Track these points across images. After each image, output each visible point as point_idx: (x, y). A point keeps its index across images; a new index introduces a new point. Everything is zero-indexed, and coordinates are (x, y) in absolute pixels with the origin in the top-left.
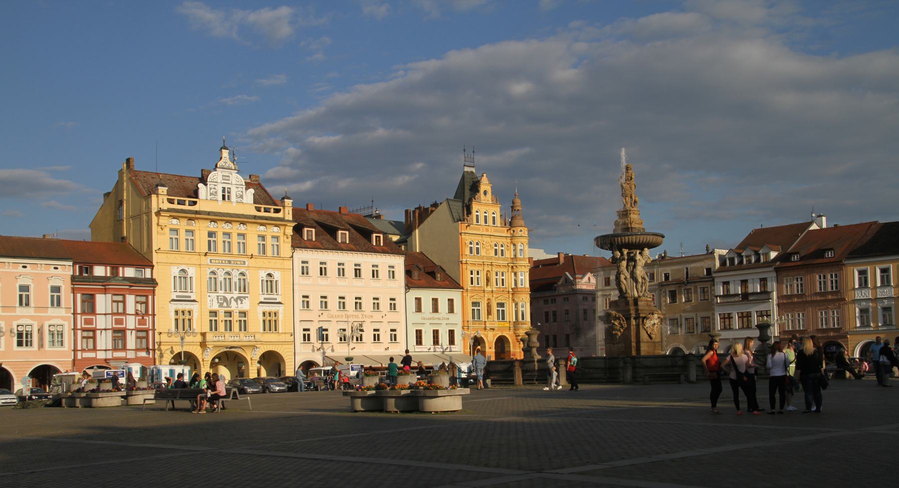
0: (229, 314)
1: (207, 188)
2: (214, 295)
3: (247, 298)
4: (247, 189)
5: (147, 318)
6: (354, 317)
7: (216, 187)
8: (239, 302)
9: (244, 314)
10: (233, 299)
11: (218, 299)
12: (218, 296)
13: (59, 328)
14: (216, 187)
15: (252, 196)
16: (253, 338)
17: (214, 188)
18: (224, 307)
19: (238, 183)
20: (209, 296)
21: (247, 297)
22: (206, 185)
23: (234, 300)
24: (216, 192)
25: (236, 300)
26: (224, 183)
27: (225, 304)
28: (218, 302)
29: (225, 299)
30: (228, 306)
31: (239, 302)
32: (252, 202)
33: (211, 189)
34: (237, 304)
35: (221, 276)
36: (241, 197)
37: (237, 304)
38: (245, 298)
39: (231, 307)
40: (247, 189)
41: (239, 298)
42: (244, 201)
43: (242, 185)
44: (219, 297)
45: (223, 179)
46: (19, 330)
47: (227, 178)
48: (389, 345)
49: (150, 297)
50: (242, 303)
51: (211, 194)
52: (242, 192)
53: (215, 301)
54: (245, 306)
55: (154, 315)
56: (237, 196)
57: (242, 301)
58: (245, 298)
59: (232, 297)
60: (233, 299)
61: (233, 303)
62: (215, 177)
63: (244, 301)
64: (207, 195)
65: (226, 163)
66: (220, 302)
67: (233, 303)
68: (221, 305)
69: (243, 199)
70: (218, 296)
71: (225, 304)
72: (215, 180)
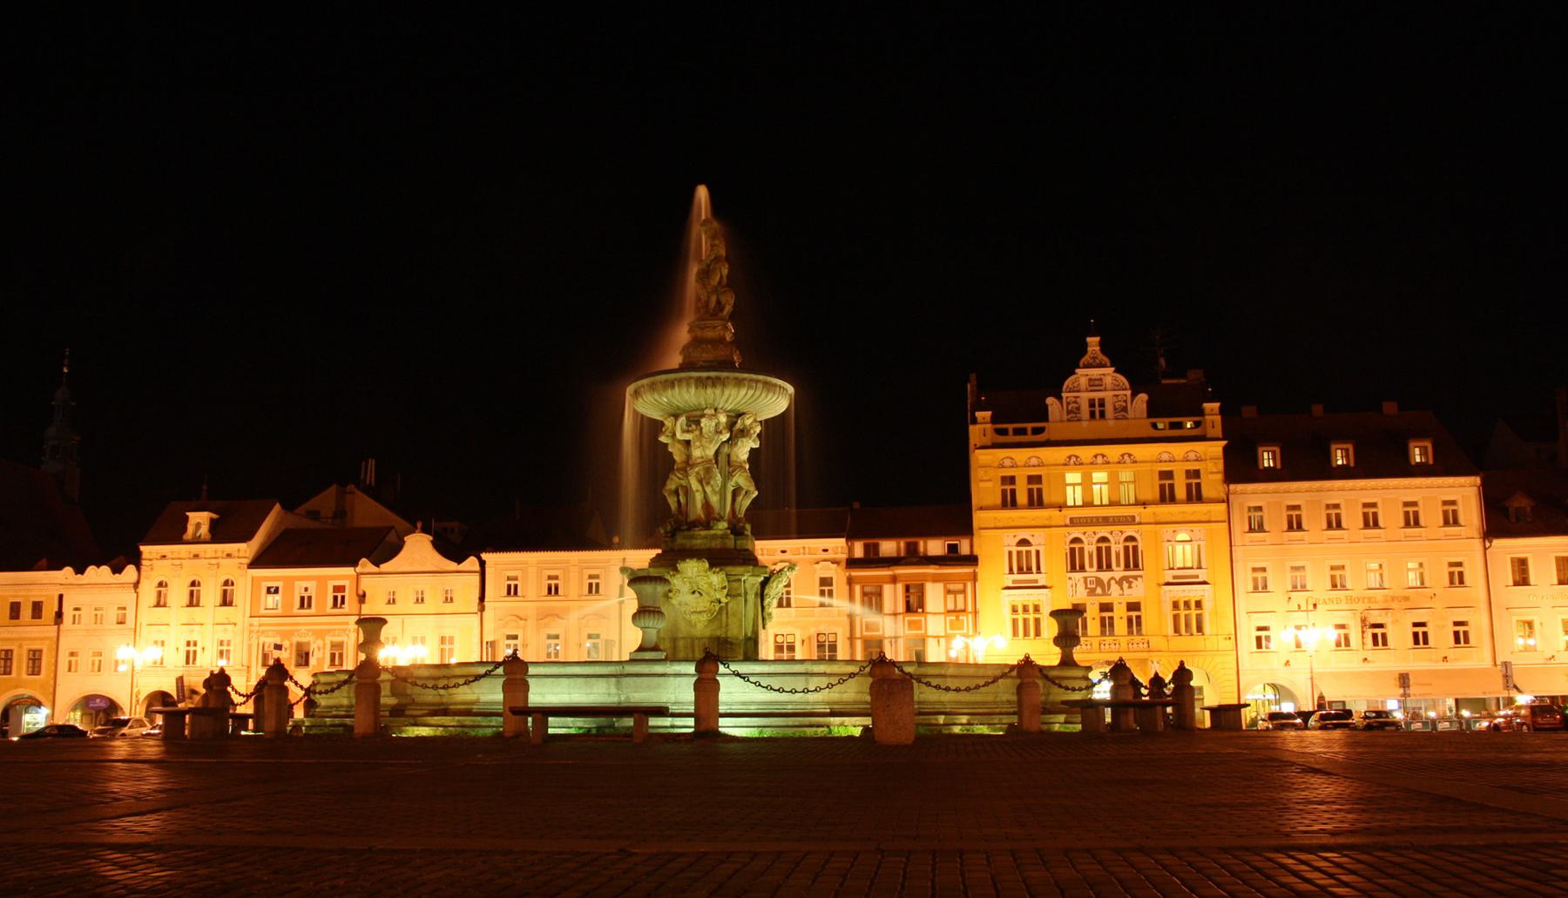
0: (1106, 607)
1: (1062, 403)
2: (1078, 576)
3: (1139, 579)
4: (1134, 395)
5: (965, 618)
6: (1366, 601)
7: (1078, 400)
8: (1125, 585)
9: (1133, 606)
10: (1113, 582)
11: (1085, 582)
12: (1085, 578)
13: (790, 639)
14: (1078, 400)
15: (1145, 405)
16: (1146, 645)
17: (1075, 402)
18: (1098, 595)
19: (1117, 388)
20: (1070, 578)
21: (1141, 576)
22: (1060, 398)
23: (1116, 582)
24: (1078, 409)
25: (1120, 583)
26: (1092, 391)
27: (1099, 591)
28: (1086, 588)
29: (1099, 582)
30: (1104, 593)
31: (1125, 585)
32: (1145, 415)
33: (1068, 404)
34: (1122, 589)
35: (1090, 547)
36: (1125, 409)
37: (1122, 589)
38: (1136, 578)
39: (1110, 595)
40: (1134, 395)
41: (1124, 578)
42: (1131, 414)
43: (1126, 389)
44: (1089, 579)
45: (1090, 386)
46: (820, 640)
47: (1097, 383)
48: (1451, 654)
49: (969, 585)
50: (1130, 587)
51: (1069, 412)
52: (1125, 401)
53: (1081, 588)
54: (1136, 593)
55: (975, 612)
56: (1115, 409)
57: (1130, 583)
58: (1136, 578)
59: (1113, 578)
60: (1113, 582)
61: (1114, 587)
62: (1076, 385)
63: (1135, 583)
64: (1061, 415)
65: (1094, 358)
66: (1089, 586)
67: (1114, 587)
68: (1092, 592)
69: (1127, 412)
70: (1085, 578)
71: (1099, 591)
72: (1076, 389)
